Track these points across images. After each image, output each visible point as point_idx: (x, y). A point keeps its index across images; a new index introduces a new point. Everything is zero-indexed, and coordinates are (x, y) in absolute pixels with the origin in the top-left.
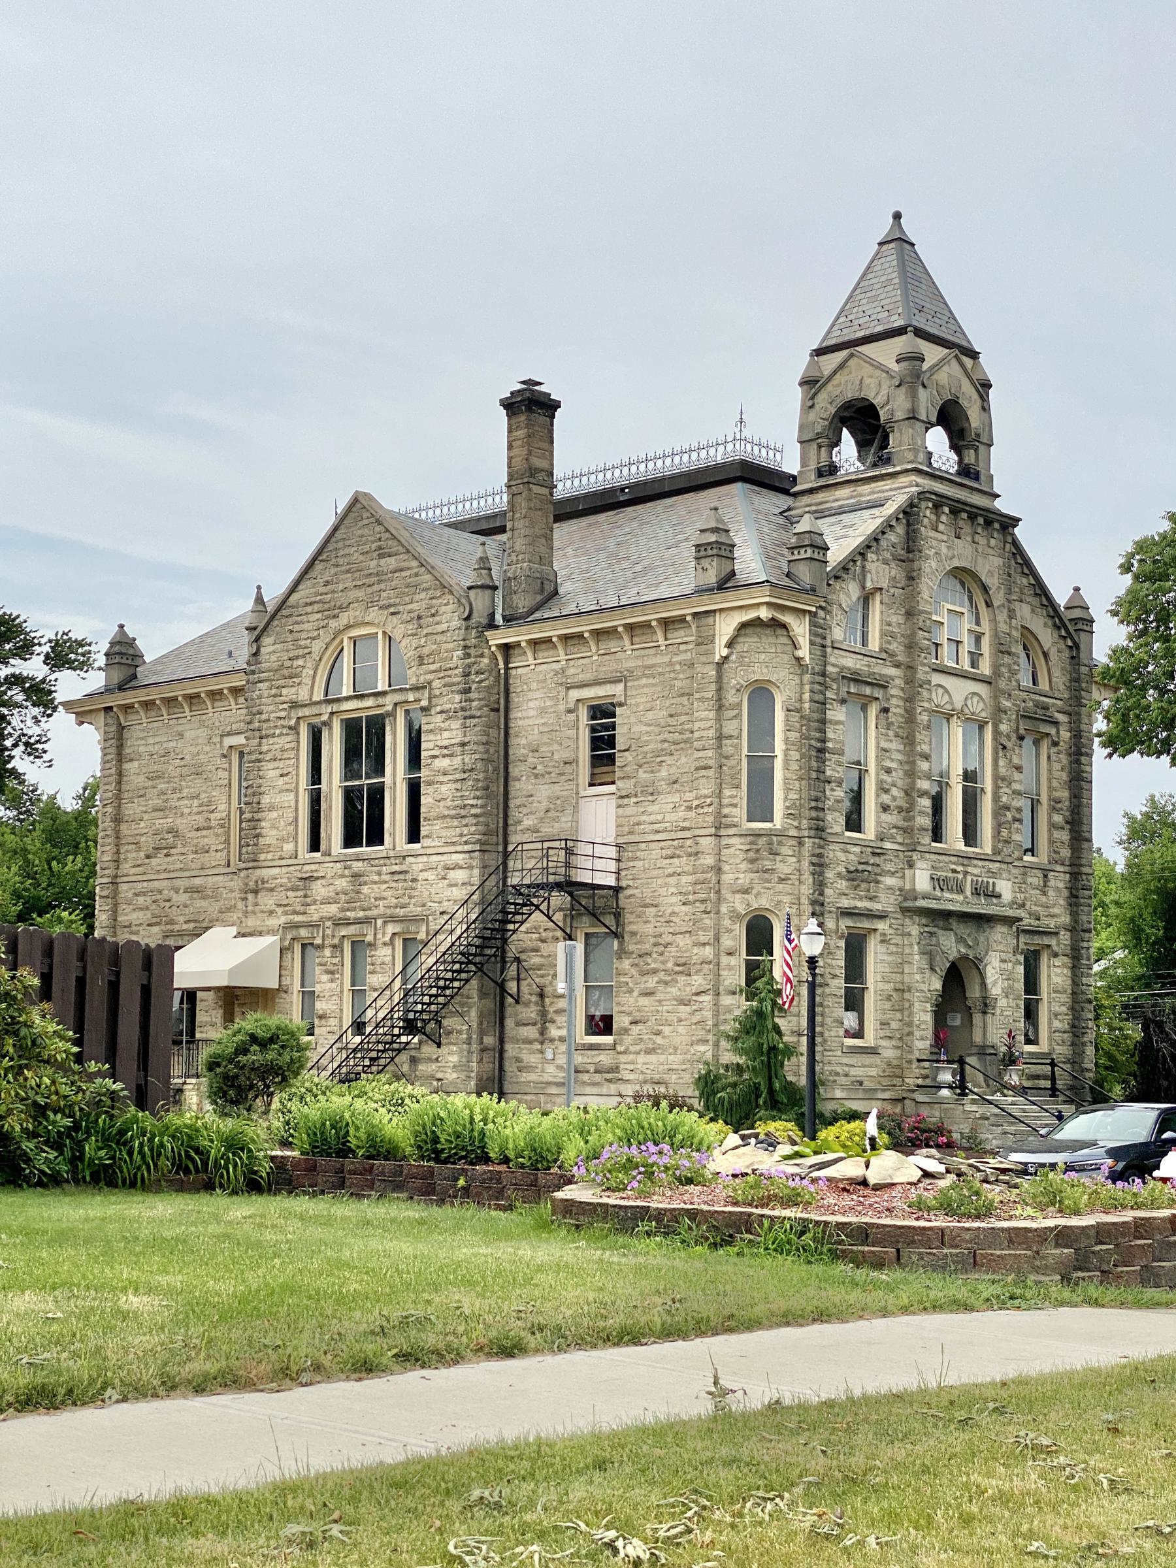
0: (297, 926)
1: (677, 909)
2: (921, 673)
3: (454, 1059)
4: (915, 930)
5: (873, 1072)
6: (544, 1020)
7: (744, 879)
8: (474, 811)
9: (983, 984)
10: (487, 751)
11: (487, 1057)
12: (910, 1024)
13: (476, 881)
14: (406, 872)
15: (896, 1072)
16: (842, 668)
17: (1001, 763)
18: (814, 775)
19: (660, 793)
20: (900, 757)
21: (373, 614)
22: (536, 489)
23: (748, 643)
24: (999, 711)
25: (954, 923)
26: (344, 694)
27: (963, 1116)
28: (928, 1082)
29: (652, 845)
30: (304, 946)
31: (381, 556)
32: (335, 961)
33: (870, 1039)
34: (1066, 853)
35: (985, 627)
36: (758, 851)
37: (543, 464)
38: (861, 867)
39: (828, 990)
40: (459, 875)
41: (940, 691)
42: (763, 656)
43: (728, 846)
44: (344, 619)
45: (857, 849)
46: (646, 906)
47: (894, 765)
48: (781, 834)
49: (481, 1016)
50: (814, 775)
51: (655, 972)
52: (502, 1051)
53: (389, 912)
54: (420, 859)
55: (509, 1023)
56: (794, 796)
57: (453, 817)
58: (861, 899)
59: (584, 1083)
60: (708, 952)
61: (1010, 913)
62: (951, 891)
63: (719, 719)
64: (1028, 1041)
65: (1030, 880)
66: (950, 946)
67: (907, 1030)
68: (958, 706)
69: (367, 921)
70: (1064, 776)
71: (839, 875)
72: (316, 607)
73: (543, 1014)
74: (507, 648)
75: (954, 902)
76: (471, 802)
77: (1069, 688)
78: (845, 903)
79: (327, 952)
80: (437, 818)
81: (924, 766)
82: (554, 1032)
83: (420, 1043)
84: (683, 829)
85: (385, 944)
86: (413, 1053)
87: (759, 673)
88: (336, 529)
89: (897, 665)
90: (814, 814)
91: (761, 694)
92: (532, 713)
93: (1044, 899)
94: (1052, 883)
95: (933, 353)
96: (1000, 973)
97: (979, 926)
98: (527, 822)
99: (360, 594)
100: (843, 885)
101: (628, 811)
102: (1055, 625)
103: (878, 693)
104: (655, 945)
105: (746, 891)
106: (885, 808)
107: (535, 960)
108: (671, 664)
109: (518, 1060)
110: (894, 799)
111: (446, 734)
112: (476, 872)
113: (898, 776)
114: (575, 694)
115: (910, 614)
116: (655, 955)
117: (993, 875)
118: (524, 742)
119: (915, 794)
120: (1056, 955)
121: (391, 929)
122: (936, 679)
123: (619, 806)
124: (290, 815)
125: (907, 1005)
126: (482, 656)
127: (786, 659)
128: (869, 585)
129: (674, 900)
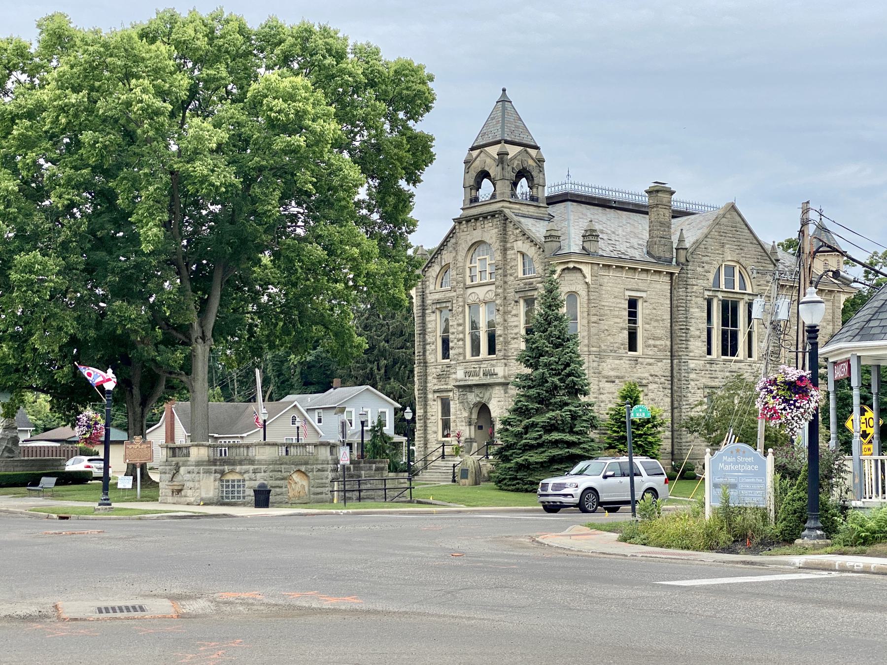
66: (472, 398)
68: (482, 298)
78: (436, 387)
95: (513, 151)
117: (493, 366)
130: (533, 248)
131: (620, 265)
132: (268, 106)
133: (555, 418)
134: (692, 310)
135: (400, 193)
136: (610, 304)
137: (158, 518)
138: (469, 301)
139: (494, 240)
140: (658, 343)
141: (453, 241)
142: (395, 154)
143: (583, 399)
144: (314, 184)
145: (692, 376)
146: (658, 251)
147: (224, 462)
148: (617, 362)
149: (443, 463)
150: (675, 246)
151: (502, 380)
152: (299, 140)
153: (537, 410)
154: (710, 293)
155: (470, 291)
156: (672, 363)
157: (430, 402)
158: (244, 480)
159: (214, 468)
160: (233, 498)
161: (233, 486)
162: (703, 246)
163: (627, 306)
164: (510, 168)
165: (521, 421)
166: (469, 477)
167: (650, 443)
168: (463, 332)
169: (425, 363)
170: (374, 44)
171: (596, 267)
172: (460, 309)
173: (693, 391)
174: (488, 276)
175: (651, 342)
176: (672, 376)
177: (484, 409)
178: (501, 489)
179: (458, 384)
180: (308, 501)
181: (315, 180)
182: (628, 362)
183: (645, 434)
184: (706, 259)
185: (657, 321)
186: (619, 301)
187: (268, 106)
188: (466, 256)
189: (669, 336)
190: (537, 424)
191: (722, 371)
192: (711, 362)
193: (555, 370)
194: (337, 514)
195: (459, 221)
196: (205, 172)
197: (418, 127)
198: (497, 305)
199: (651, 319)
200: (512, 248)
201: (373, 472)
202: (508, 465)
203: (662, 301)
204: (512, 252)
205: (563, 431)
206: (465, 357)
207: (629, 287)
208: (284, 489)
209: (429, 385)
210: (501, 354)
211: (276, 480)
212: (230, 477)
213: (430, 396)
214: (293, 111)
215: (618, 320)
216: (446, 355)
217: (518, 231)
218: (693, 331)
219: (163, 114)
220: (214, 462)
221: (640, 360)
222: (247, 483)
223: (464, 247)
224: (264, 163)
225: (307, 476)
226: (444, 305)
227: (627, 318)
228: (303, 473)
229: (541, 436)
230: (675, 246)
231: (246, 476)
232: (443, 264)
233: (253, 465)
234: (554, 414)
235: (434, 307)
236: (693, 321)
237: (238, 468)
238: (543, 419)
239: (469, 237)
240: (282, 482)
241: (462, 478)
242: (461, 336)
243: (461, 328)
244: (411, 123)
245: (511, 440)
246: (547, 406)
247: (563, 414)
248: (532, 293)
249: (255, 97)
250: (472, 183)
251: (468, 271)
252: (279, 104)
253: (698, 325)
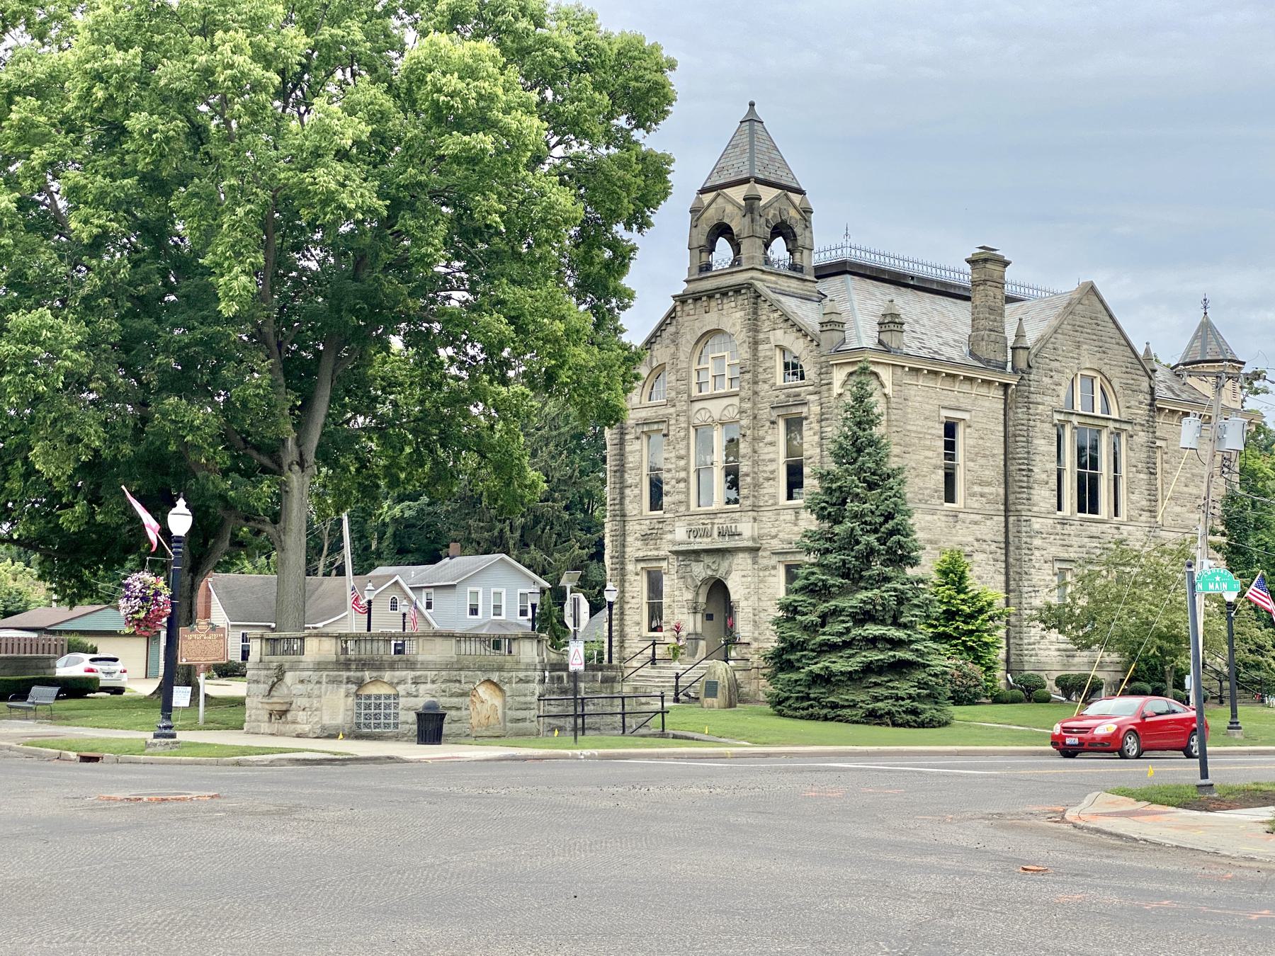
41: (703, 412)
66: (700, 570)
68: (716, 417)
78: (640, 554)
100: (639, 544)
117: (735, 521)
130: (801, 340)
131: (932, 369)
132: (434, 85)
133: (872, 601)
134: (1036, 441)
135: (615, 245)
136: (919, 429)
137: (272, 763)
138: (696, 421)
139: (738, 327)
140: (986, 490)
141: (671, 329)
142: (619, 179)
143: (910, 572)
144: (502, 214)
145: (1037, 542)
146: (985, 350)
147: (363, 664)
148: (929, 518)
149: (654, 672)
150: (1010, 344)
151: (750, 544)
152: (485, 141)
153: (841, 587)
154: (1062, 417)
155: (698, 405)
156: (1006, 522)
157: (630, 577)
158: (397, 696)
159: (345, 674)
160: (377, 726)
161: (378, 706)
162: (1051, 346)
163: (942, 433)
164: (763, 220)
165: (814, 606)
166: (719, 694)
167: (986, 644)
168: (686, 469)
169: (624, 516)
170: (587, 7)
171: (899, 371)
172: (682, 434)
173: (1037, 565)
174: (727, 382)
175: (977, 489)
176: (1007, 543)
177: (718, 589)
178: (781, 714)
179: (676, 548)
180: (502, 733)
181: (504, 208)
182: (944, 518)
183: (977, 631)
184: (1056, 364)
185: (985, 456)
186: (930, 424)
187: (434, 85)
188: (693, 352)
189: (1002, 480)
190: (843, 610)
191: (1078, 536)
192: (1063, 522)
193: (870, 524)
194: (575, 757)
195: (682, 299)
196: (333, 186)
197: (649, 141)
198: (741, 427)
199: (977, 454)
200: (767, 341)
201: (598, 685)
202: (794, 676)
203: (991, 426)
204: (767, 346)
205: (883, 622)
206: (688, 508)
207: (946, 404)
208: (464, 713)
209: (628, 550)
210: (748, 502)
211: (451, 696)
212: (373, 690)
213: (630, 567)
214: (474, 95)
215: (930, 454)
216: (656, 503)
217: (776, 315)
218: (1038, 474)
219: (264, 89)
220: (346, 665)
221: (961, 515)
222: (402, 701)
223: (688, 338)
224: (423, 178)
225: (501, 690)
226: (655, 427)
227: (942, 451)
228: (495, 684)
229: (848, 630)
230: (1010, 344)
231: (401, 689)
232: (654, 365)
233: (413, 669)
234: (870, 594)
235: (639, 430)
236: (1037, 458)
237: (387, 675)
238: (854, 603)
239: (697, 324)
240: (460, 699)
241: (707, 696)
242: (683, 475)
243: (682, 463)
244: (638, 134)
245: (799, 635)
246: (855, 582)
247: (885, 595)
248: (799, 409)
249: (412, 71)
250: (702, 243)
251: (694, 374)
252: (453, 82)
253: (1044, 466)
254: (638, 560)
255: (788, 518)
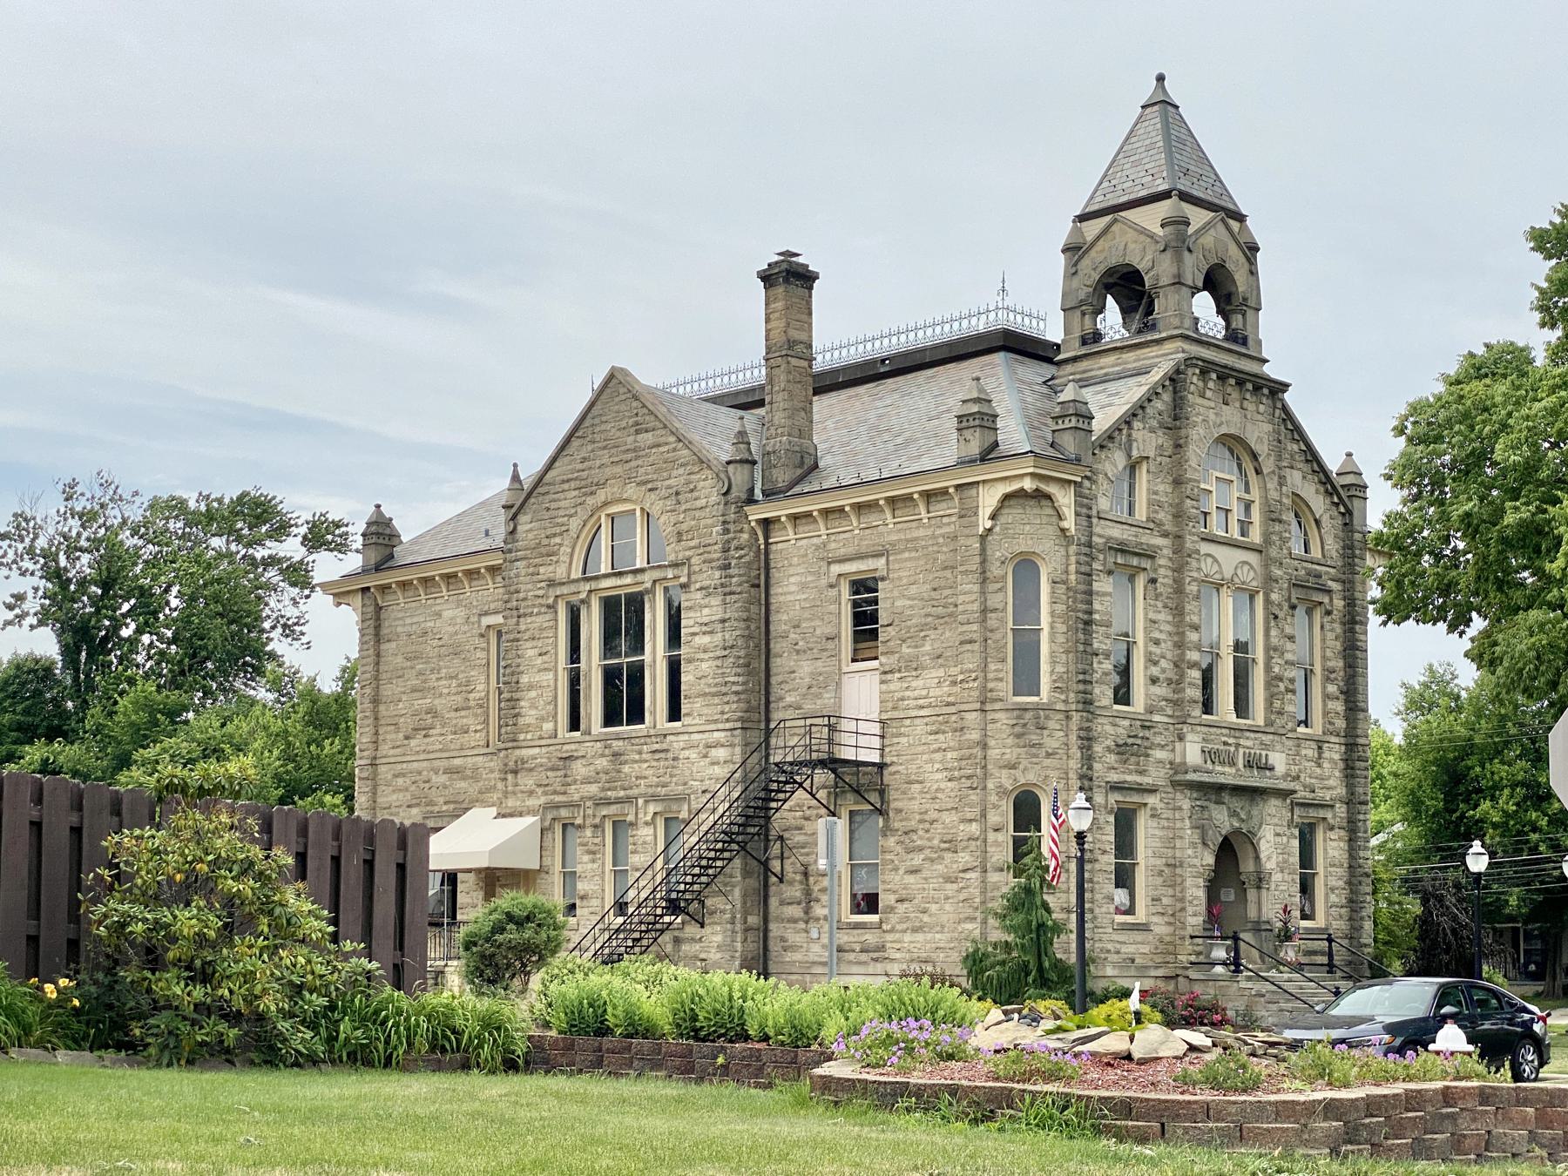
0: (557, 807)
1: (943, 786)
2: (1190, 542)
3: (719, 938)
4: (1186, 805)
5: (1145, 949)
6: (809, 899)
7: (1011, 755)
8: (735, 688)
9: (1257, 858)
10: (748, 628)
11: (751, 936)
12: (1182, 900)
13: (738, 759)
14: (667, 751)
15: (1168, 949)
16: (1109, 539)
17: (1273, 633)
18: (1081, 648)
19: (924, 669)
20: (1168, 628)
21: (631, 491)
22: (794, 361)
23: (1011, 515)
24: (1269, 581)
25: (1226, 797)
26: (603, 571)
27: (1236, 994)
28: (1202, 959)
29: (917, 721)
30: (565, 826)
31: (637, 432)
32: (596, 841)
33: (1141, 916)
34: (1341, 724)
35: (1255, 494)
36: (1025, 725)
37: (803, 336)
38: (1130, 741)
39: (1097, 866)
40: (721, 753)
41: (1209, 560)
42: (1028, 527)
43: (994, 721)
44: (601, 496)
45: (1126, 723)
46: (910, 783)
47: (1162, 636)
48: (1048, 708)
49: (745, 896)
50: (1081, 648)
51: (921, 849)
52: (766, 931)
53: (650, 791)
54: (682, 737)
55: (773, 902)
56: (1060, 669)
57: (714, 695)
58: (1130, 773)
59: (850, 962)
60: (974, 828)
61: (1283, 785)
62: (1222, 763)
63: (983, 593)
64: (1304, 917)
65: (1304, 752)
66: (1222, 819)
67: (1179, 906)
68: (1228, 575)
69: (628, 800)
70: (1338, 646)
71: (1109, 749)
72: (573, 484)
73: (808, 892)
74: (766, 523)
75: (1226, 775)
76: (732, 679)
77: (1343, 556)
78: (1114, 777)
79: (588, 832)
80: (699, 696)
81: (1193, 636)
82: (819, 911)
83: (683, 923)
84: (948, 704)
85: (646, 823)
86: (676, 933)
87: (1023, 545)
88: (592, 405)
89: (1165, 535)
90: (1081, 687)
91: (1026, 566)
92: (793, 588)
93: (1318, 770)
94: (1326, 754)
95: (1197, 217)
96: (1274, 846)
97: (1252, 800)
98: (789, 699)
99: (618, 470)
100: (1112, 758)
101: (892, 687)
102: (1326, 491)
103: (1146, 564)
104: (921, 821)
105: (1013, 767)
106: (1154, 681)
107: (799, 838)
108: (934, 537)
109: (783, 939)
110: (1163, 671)
111: (706, 611)
112: (738, 750)
113: (1166, 647)
114: (836, 569)
115: (1178, 482)
116: (921, 833)
118: (785, 617)
119: (1184, 666)
120: (1332, 828)
121: (652, 808)
122: (1205, 548)
123: (882, 682)
124: (548, 695)
125: (1179, 880)
126: (741, 531)
127: (1052, 530)
128: (1135, 453)
129: (939, 776)
209: (1097, 766)
254: (1115, 787)
255: (1310, 753)
